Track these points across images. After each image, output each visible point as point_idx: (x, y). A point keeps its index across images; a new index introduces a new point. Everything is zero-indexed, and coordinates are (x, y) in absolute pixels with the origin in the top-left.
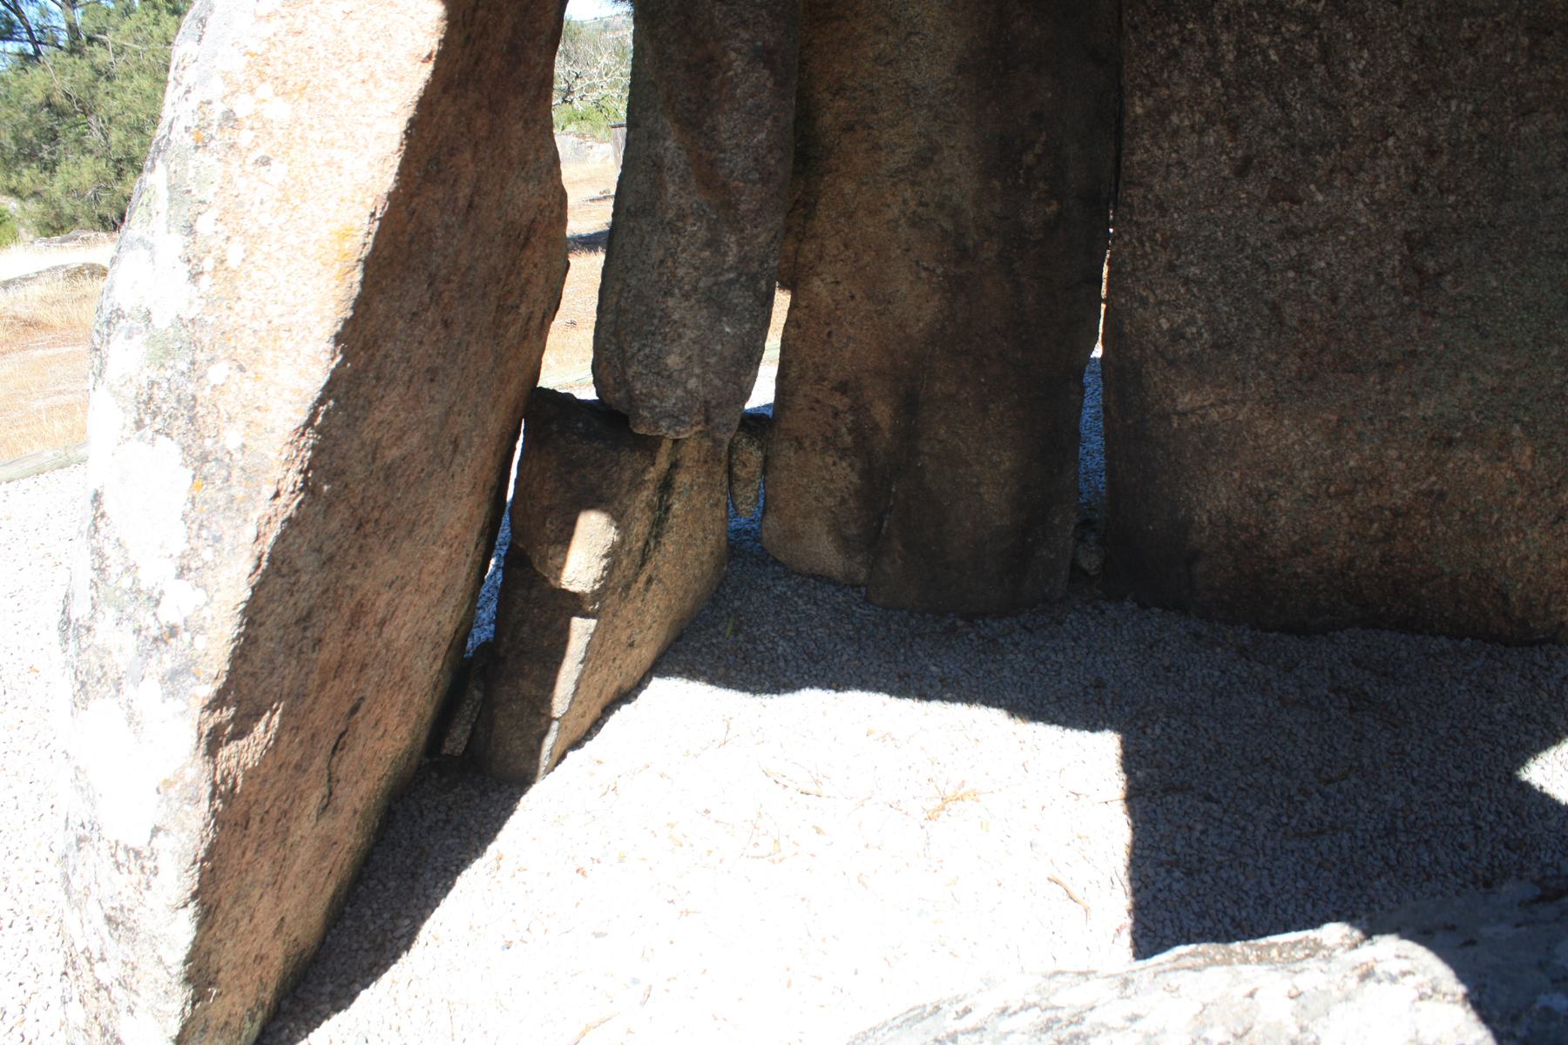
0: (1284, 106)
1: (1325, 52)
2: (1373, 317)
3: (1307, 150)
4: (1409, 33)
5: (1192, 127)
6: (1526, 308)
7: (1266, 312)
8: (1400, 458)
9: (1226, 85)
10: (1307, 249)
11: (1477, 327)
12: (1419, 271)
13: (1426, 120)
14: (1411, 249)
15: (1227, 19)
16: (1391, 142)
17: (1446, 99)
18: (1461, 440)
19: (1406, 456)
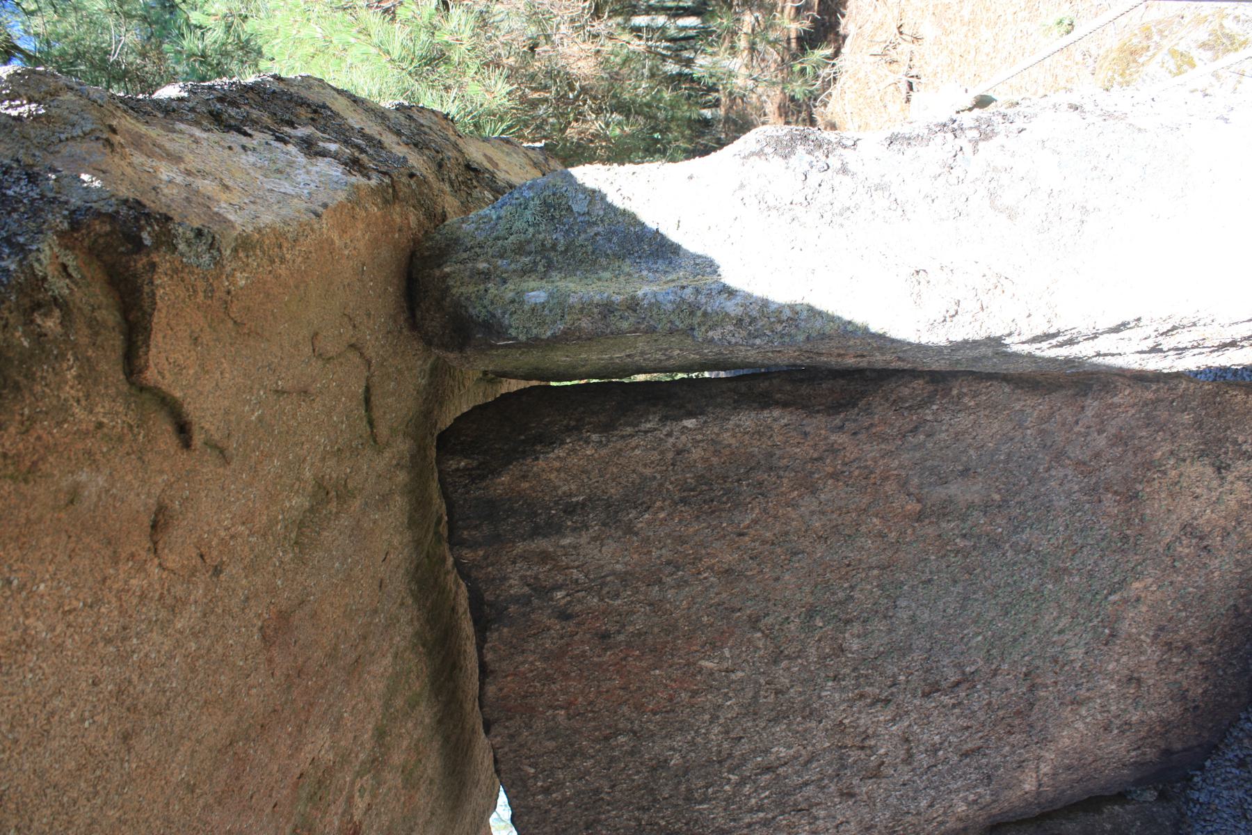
0: (806, 784)
1: (768, 769)
2: (989, 704)
3: (844, 767)
4: (764, 728)
5: (810, 824)
6: (1007, 613)
7: (968, 760)
8: (1117, 661)
9: (783, 813)
10: (922, 748)
11: (1015, 640)
12: (957, 684)
13: (834, 705)
14: (938, 691)
15: (734, 820)
16: (846, 721)
17: (820, 697)
18: (1112, 629)
19: (1116, 657)
